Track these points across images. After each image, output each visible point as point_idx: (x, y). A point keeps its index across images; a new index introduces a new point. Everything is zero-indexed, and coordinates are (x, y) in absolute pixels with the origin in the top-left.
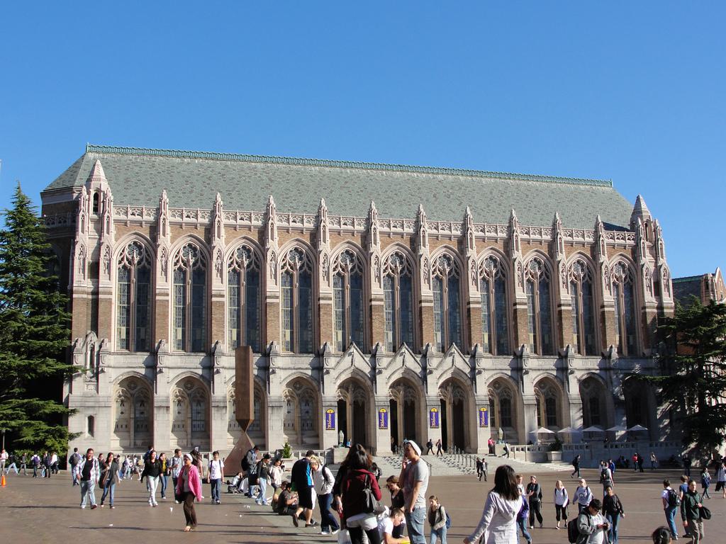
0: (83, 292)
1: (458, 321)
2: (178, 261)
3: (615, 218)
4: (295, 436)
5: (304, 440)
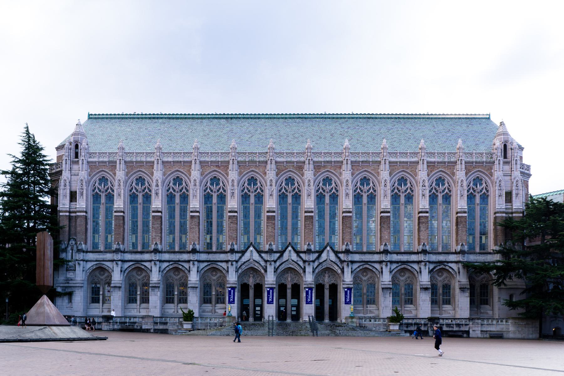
0: (66, 212)
1: (336, 227)
2: (132, 189)
3: (483, 142)
4: (211, 308)
5: (217, 310)
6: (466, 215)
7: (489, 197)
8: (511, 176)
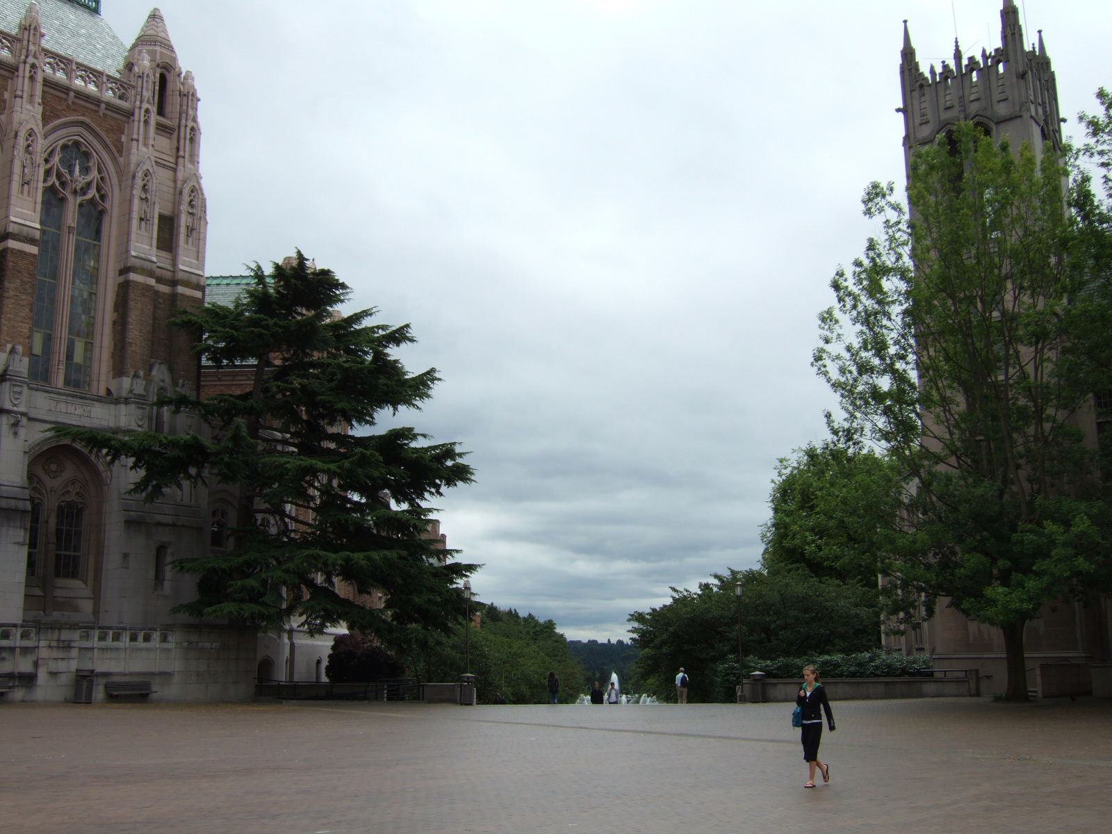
6: (34, 250)
7: (106, 220)
8: (175, 170)
